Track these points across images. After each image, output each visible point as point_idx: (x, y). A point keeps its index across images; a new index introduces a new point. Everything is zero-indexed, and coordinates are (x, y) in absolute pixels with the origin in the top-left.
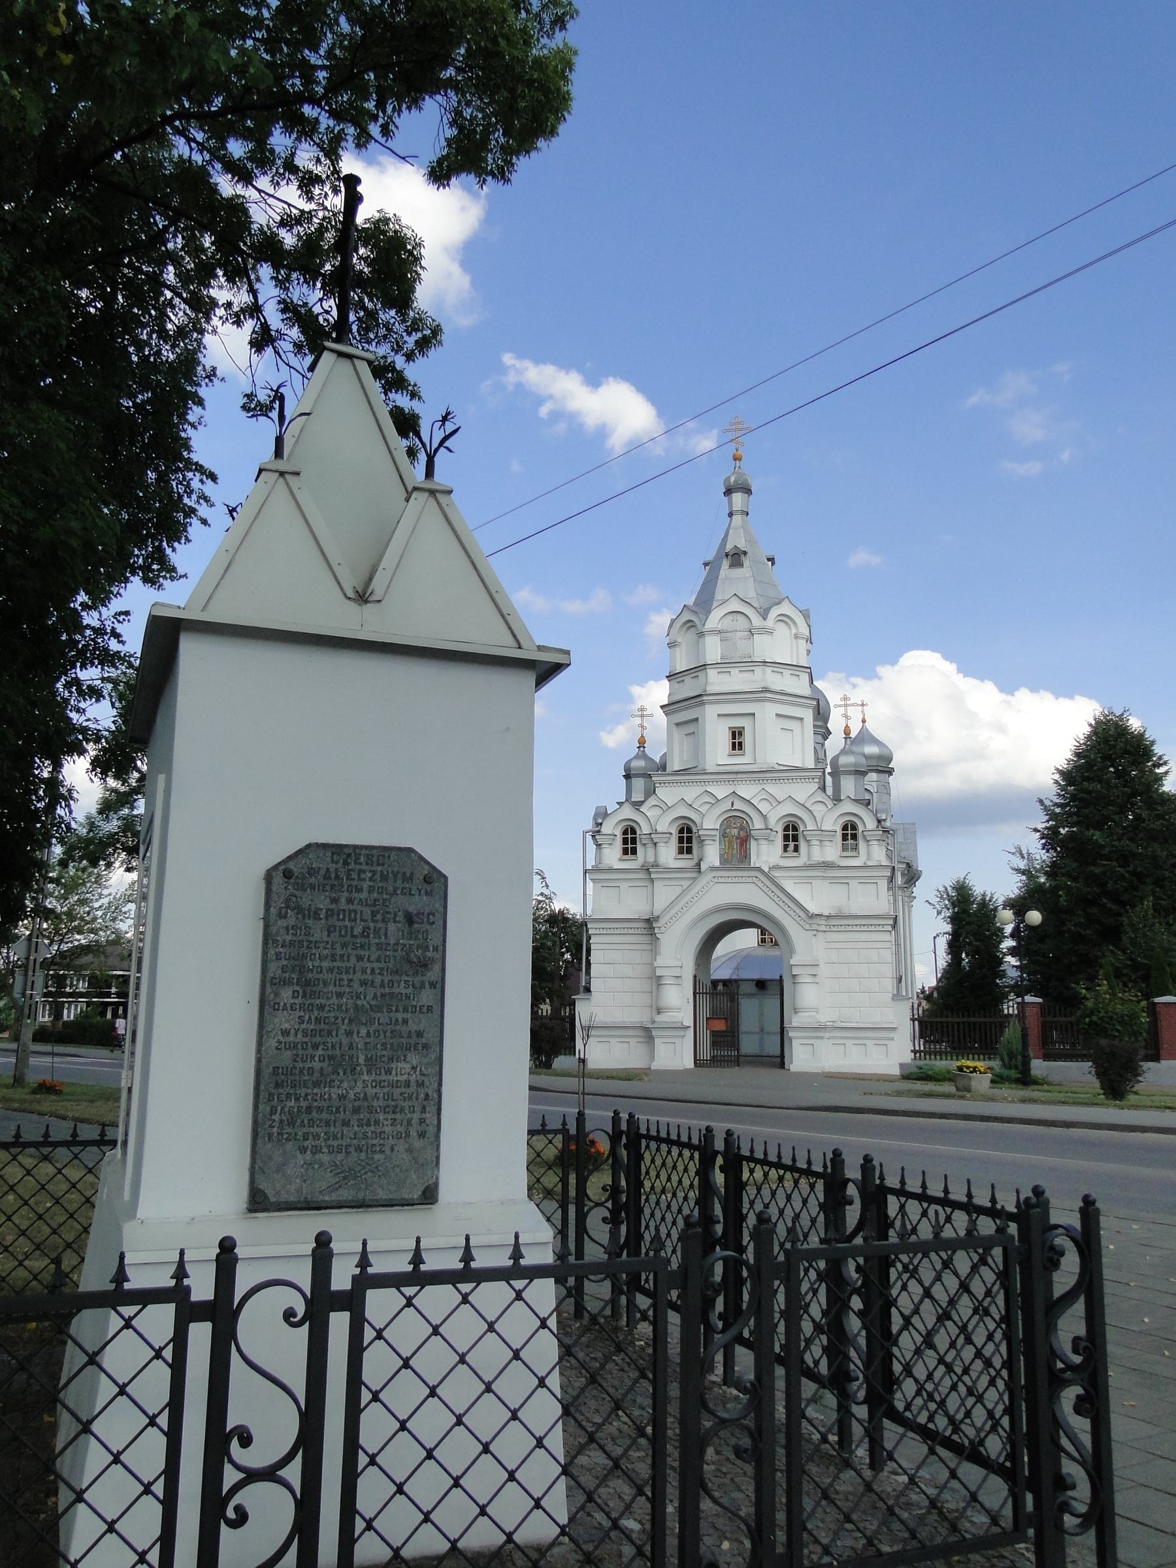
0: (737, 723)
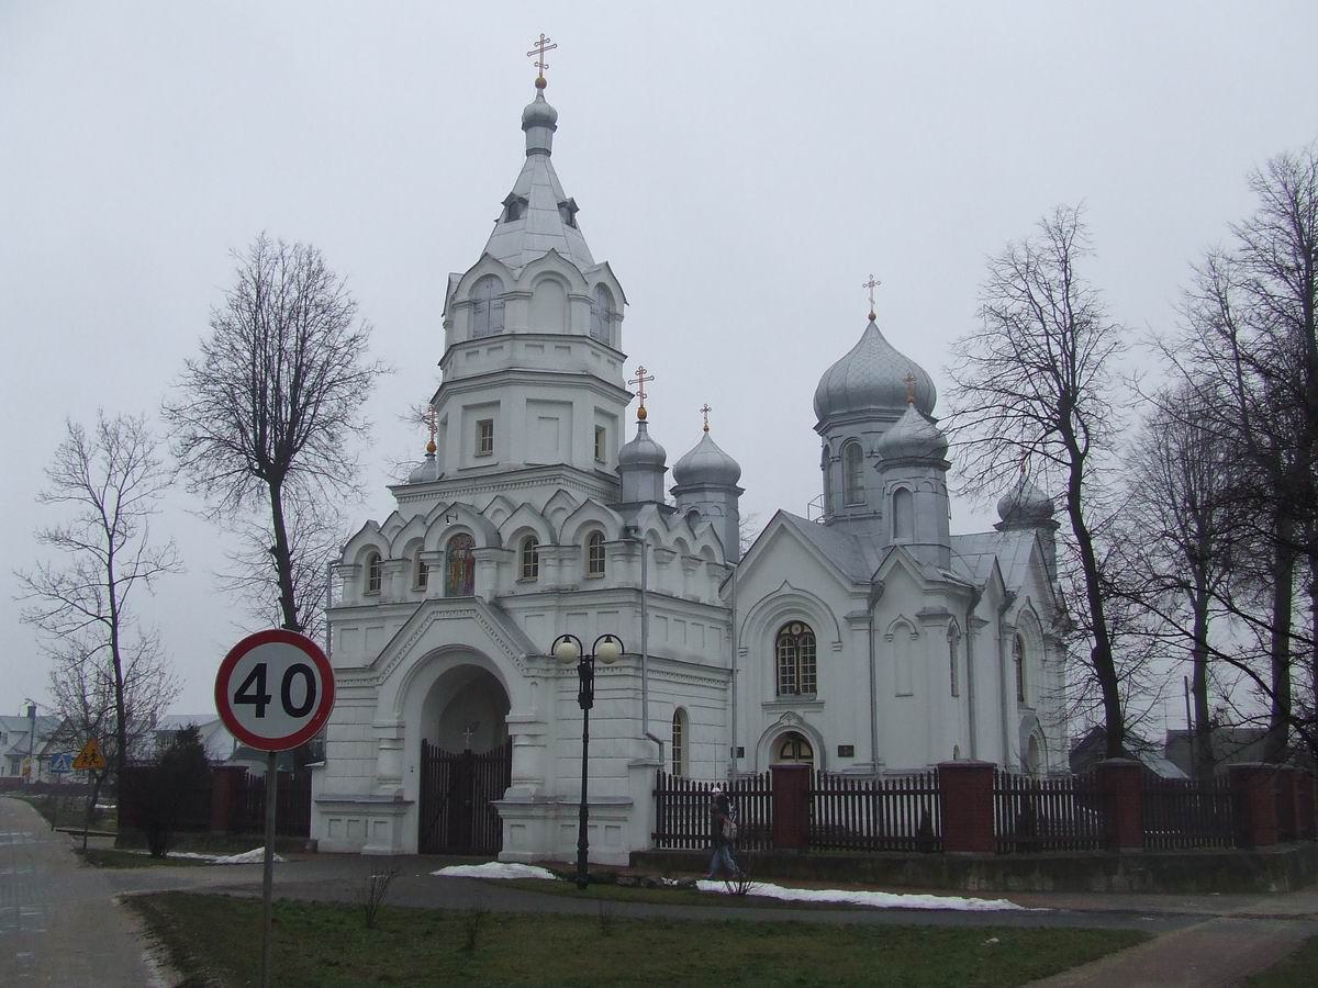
0: (484, 415)
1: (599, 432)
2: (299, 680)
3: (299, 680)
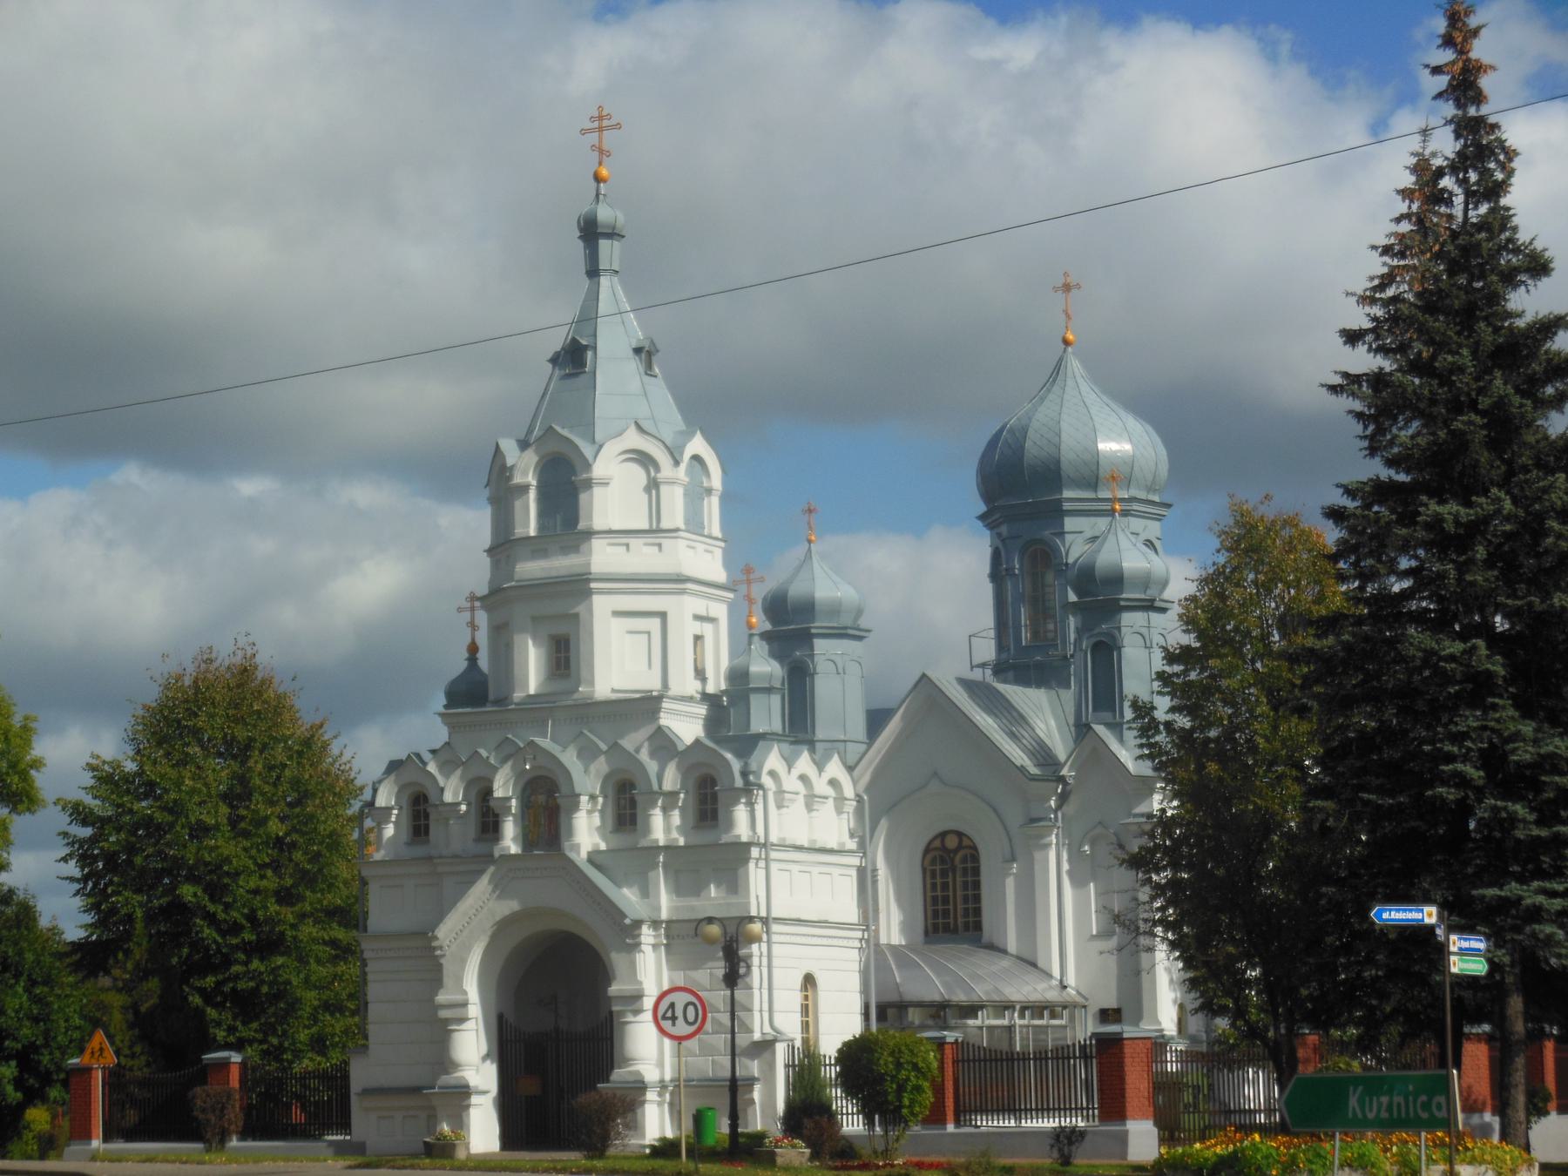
0: (560, 629)
1: (698, 639)
2: (691, 1009)
3: (691, 1009)
